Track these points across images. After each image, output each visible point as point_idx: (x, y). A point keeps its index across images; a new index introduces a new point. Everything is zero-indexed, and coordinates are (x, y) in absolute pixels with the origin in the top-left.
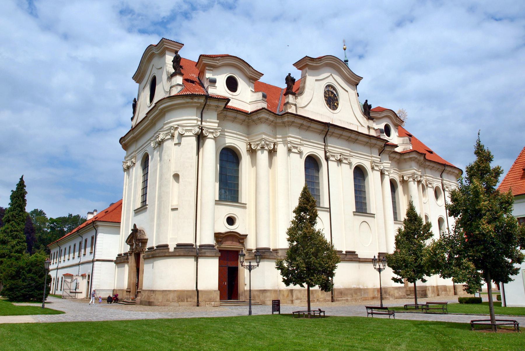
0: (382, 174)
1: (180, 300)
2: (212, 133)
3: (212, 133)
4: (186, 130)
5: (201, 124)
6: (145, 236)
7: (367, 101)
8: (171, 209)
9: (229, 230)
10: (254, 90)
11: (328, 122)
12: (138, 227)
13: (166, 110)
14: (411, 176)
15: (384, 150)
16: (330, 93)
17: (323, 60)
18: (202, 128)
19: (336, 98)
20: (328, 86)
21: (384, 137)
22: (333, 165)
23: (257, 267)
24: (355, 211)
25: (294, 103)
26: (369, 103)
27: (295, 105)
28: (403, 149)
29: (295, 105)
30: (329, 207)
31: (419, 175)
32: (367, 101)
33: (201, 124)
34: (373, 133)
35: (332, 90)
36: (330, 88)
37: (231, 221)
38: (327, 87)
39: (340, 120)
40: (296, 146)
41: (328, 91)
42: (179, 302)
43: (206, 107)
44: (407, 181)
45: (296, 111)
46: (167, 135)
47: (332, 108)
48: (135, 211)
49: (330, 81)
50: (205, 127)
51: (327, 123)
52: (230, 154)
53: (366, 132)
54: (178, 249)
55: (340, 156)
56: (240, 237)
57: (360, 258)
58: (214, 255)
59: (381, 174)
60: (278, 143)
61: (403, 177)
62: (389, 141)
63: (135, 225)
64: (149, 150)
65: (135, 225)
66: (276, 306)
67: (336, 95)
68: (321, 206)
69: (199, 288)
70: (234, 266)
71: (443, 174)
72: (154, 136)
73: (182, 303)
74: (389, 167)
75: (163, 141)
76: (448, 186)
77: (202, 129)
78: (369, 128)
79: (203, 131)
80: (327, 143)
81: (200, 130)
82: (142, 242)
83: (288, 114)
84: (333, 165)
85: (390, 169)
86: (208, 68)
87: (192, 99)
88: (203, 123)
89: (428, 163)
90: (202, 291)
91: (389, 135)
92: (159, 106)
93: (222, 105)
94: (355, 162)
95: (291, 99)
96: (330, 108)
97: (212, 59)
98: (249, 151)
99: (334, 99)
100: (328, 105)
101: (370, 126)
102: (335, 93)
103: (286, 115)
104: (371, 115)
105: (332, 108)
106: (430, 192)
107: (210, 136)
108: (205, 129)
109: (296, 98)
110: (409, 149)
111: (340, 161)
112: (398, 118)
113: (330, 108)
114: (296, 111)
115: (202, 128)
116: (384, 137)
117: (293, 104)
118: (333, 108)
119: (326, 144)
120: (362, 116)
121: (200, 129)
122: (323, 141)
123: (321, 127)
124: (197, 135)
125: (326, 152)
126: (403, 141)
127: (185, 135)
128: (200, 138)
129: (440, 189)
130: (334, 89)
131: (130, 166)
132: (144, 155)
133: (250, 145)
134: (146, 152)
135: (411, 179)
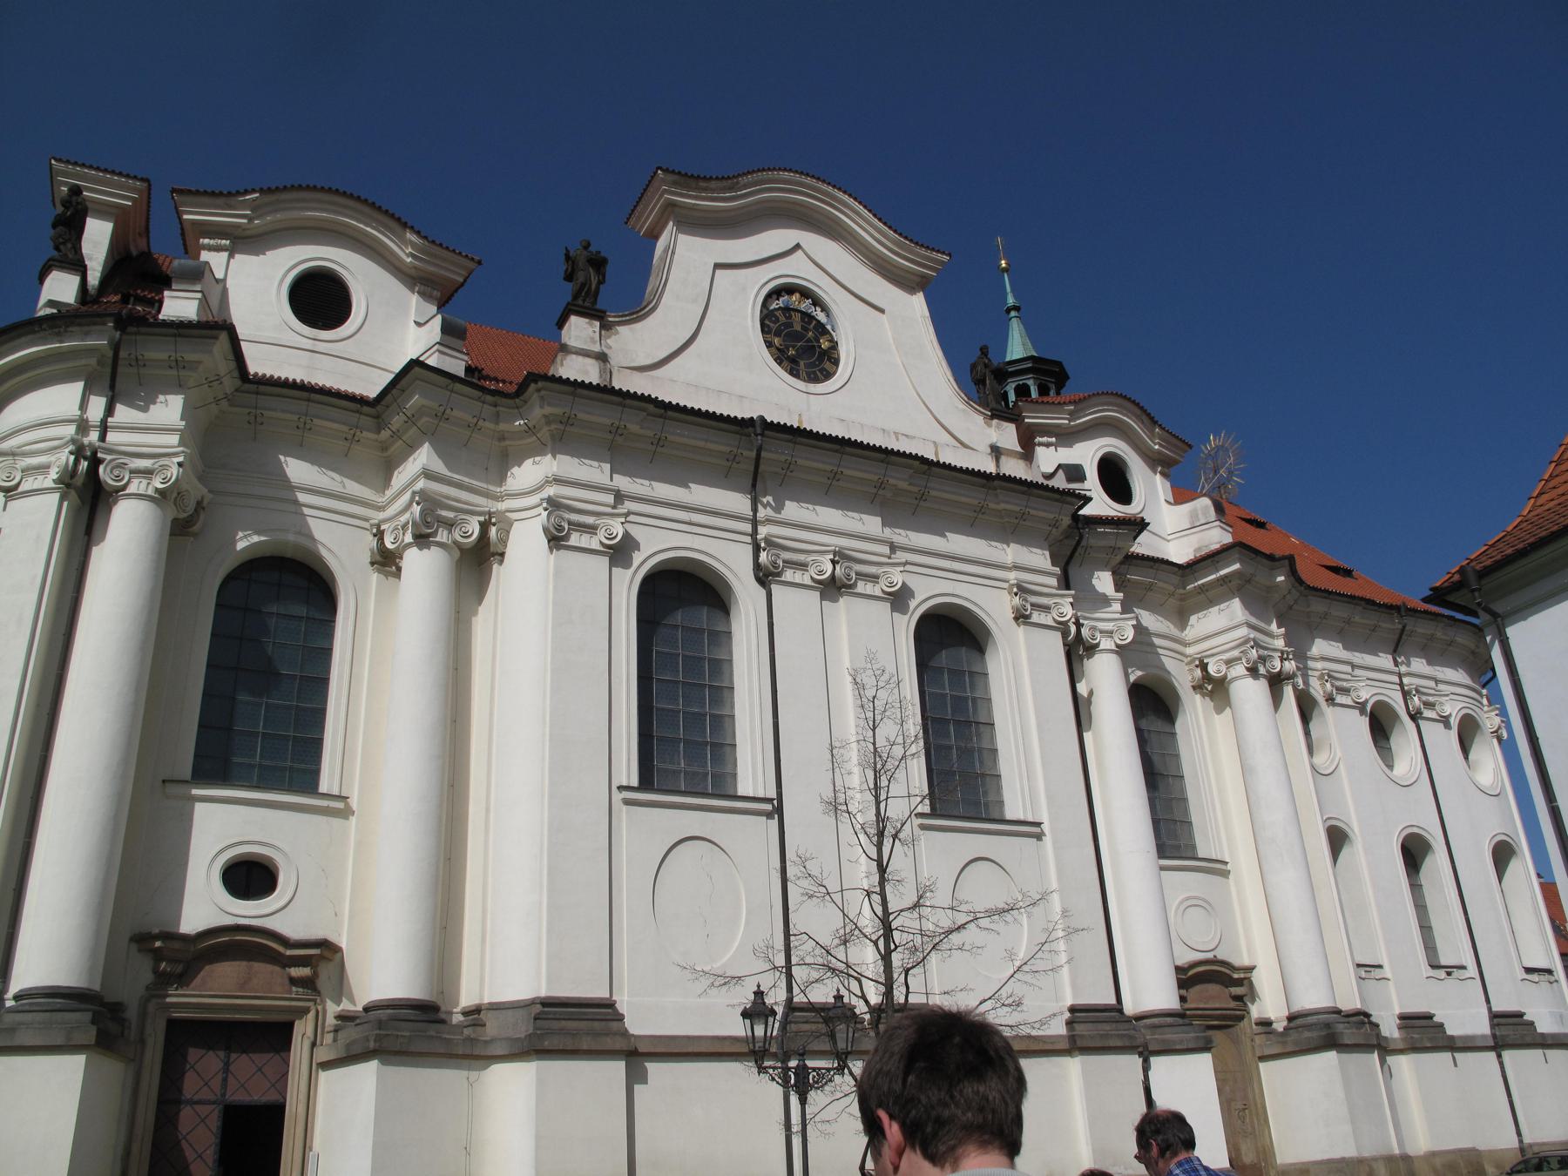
2: (148, 473)
3: (148, 473)
4: (27, 471)
5: (103, 438)
9: (229, 921)
14: (1236, 653)
15: (1078, 543)
16: (797, 318)
17: (745, 187)
18: (95, 453)
20: (789, 289)
22: (795, 604)
25: (596, 348)
27: (602, 358)
30: (772, 794)
31: (1275, 650)
33: (103, 438)
35: (805, 305)
40: (590, 520)
41: (787, 310)
43: (120, 369)
44: (1225, 677)
49: (796, 269)
50: (110, 451)
55: (834, 562)
56: (289, 952)
58: (59, 1041)
60: (513, 516)
61: (1204, 666)
67: (829, 327)
70: (258, 1094)
74: (1118, 616)
76: (1431, 699)
77: (95, 462)
81: (84, 465)
83: (540, 384)
84: (795, 604)
85: (1121, 623)
86: (206, 241)
87: (60, 336)
88: (112, 437)
89: (1318, 606)
94: (929, 591)
95: (579, 330)
97: (221, 201)
100: (785, 363)
102: (821, 317)
107: (137, 486)
108: (109, 457)
109: (606, 327)
111: (832, 588)
120: (962, 406)
123: (722, 444)
126: (1193, 515)
127: (24, 487)
133: (380, 535)
135: (1239, 670)
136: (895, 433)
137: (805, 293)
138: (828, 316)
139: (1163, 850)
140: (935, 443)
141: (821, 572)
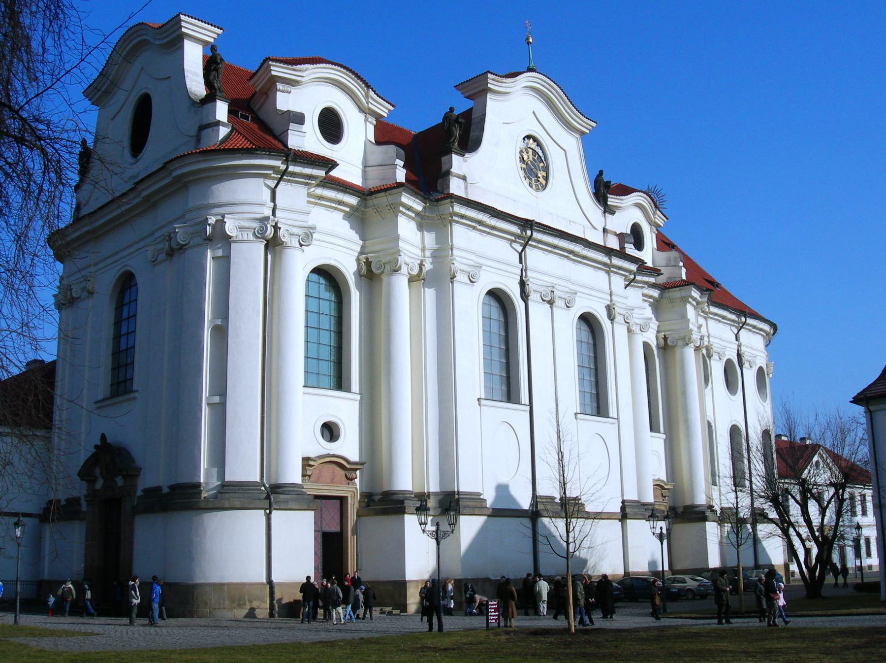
0: (629, 331)
1: (235, 605)
5: (274, 214)
6: (133, 462)
7: (601, 173)
8: (208, 404)
10: (374, 141)
11: (531, 219)
12: (109, 440)
13: (191, 178)
16: (530, 152)
18: (276, 224)
19: (542, 164)
20: (528, 137)
21: (630, 250)
23: (451, 534)
24: (579, 411)
26: (606, 178)
28: (667, 278)
29: (464, 178)
32: (601, 173)
33: (274, 214)
34: (613, 243)
36: (531, 140)
37: (330, 431)
38: (524, 139)
39: (565, 219)
42: (234, 608)
45: (467, 193)
46: (194, 237)
47: (534, 187)
48: (98, 405)
51: (529, 220)
52: (322, 281)
53: (597, 238)
54: (226, 495)
56: (348, 466)
57: (588, 513)
59: (628, 332)
62: (646, 263)
63: (103, 437)
64: (137, 264)
65: (103, 437)
66: (494, 612)
67: (543, 159)
68: (523, 403)
69: (275, 578)
71: (740, 332)
72: (152, 234)
73: (239, 610)
75: (182, 248)
77: (276, 228)
78: (605, 230)
79: (281, 233)
80: (526, 264)
82: (124, 477)
88: (278, 213)
90: (281, 584)
91: (639, 244)
92: (175, 169)
93: (321, 173)
96: (531, 187)
98: (365, 276)
99: (538, 166)
100: (527, 179)
101: (607, 227)
102: (541, 154)
103: (449, 200)
104: (609, 203)
105: (534, 187)
106: (717, 369)
110: (680, 279)
112: (658, 212)
113: (530, 185)
114: (467, 193)
115: (276, 224)
116: (630, 250)
117: (459, 177)
118: (536, 185)
119: (524, 266)
121: (274, 227)
122: (518, 261)
124: (266, 241)
125: (523, 284)
126: (669, 260)
128: (273, 245)
129: (735, 366)
130: (539, 144)
131: (78, 298)
132: (122, 276)
134: (128, 268)
136: (570, 221)
137: (535, 140)
138: (543, 152)
139: (651, 430)
140: (583, 226)
141: (545, 296)
